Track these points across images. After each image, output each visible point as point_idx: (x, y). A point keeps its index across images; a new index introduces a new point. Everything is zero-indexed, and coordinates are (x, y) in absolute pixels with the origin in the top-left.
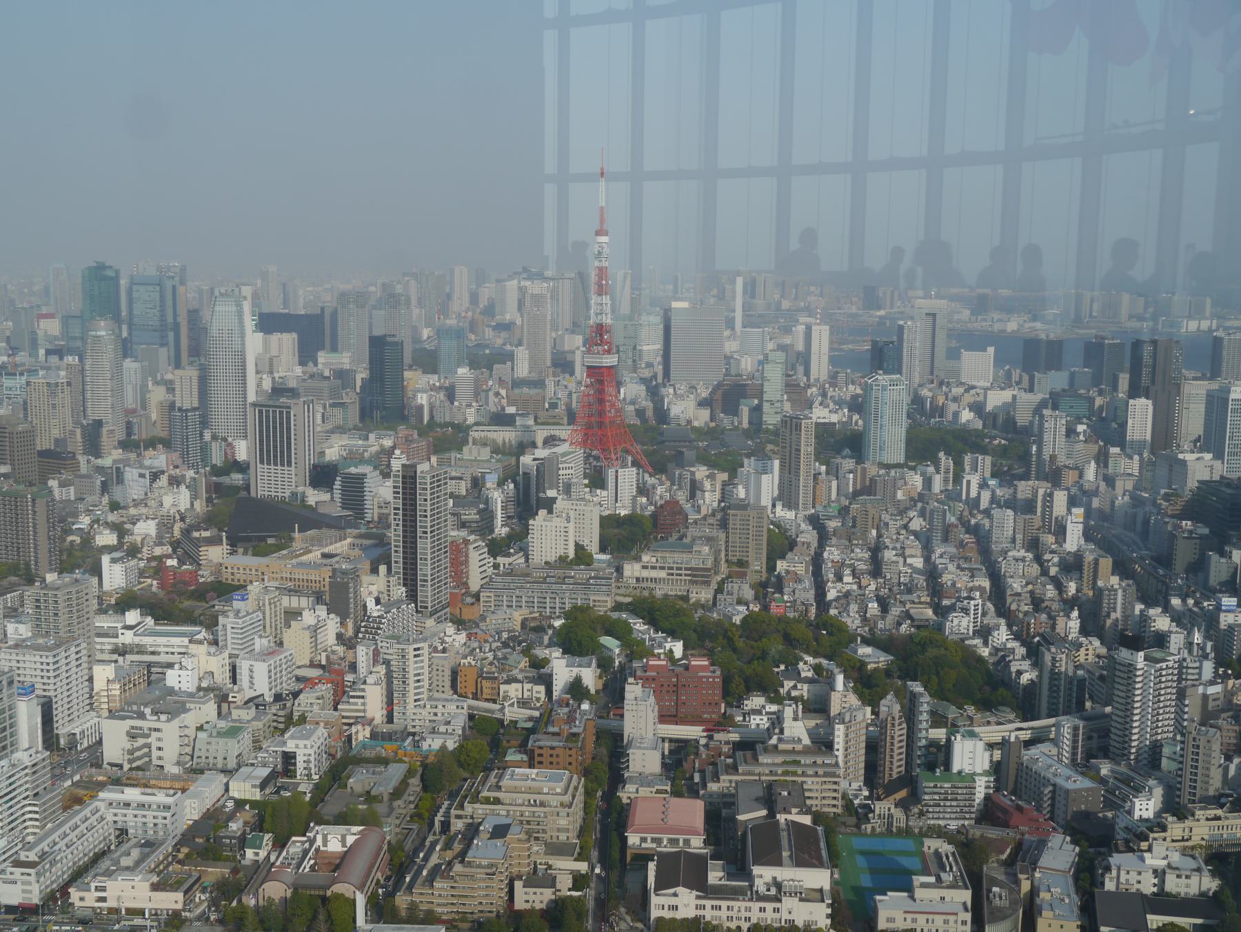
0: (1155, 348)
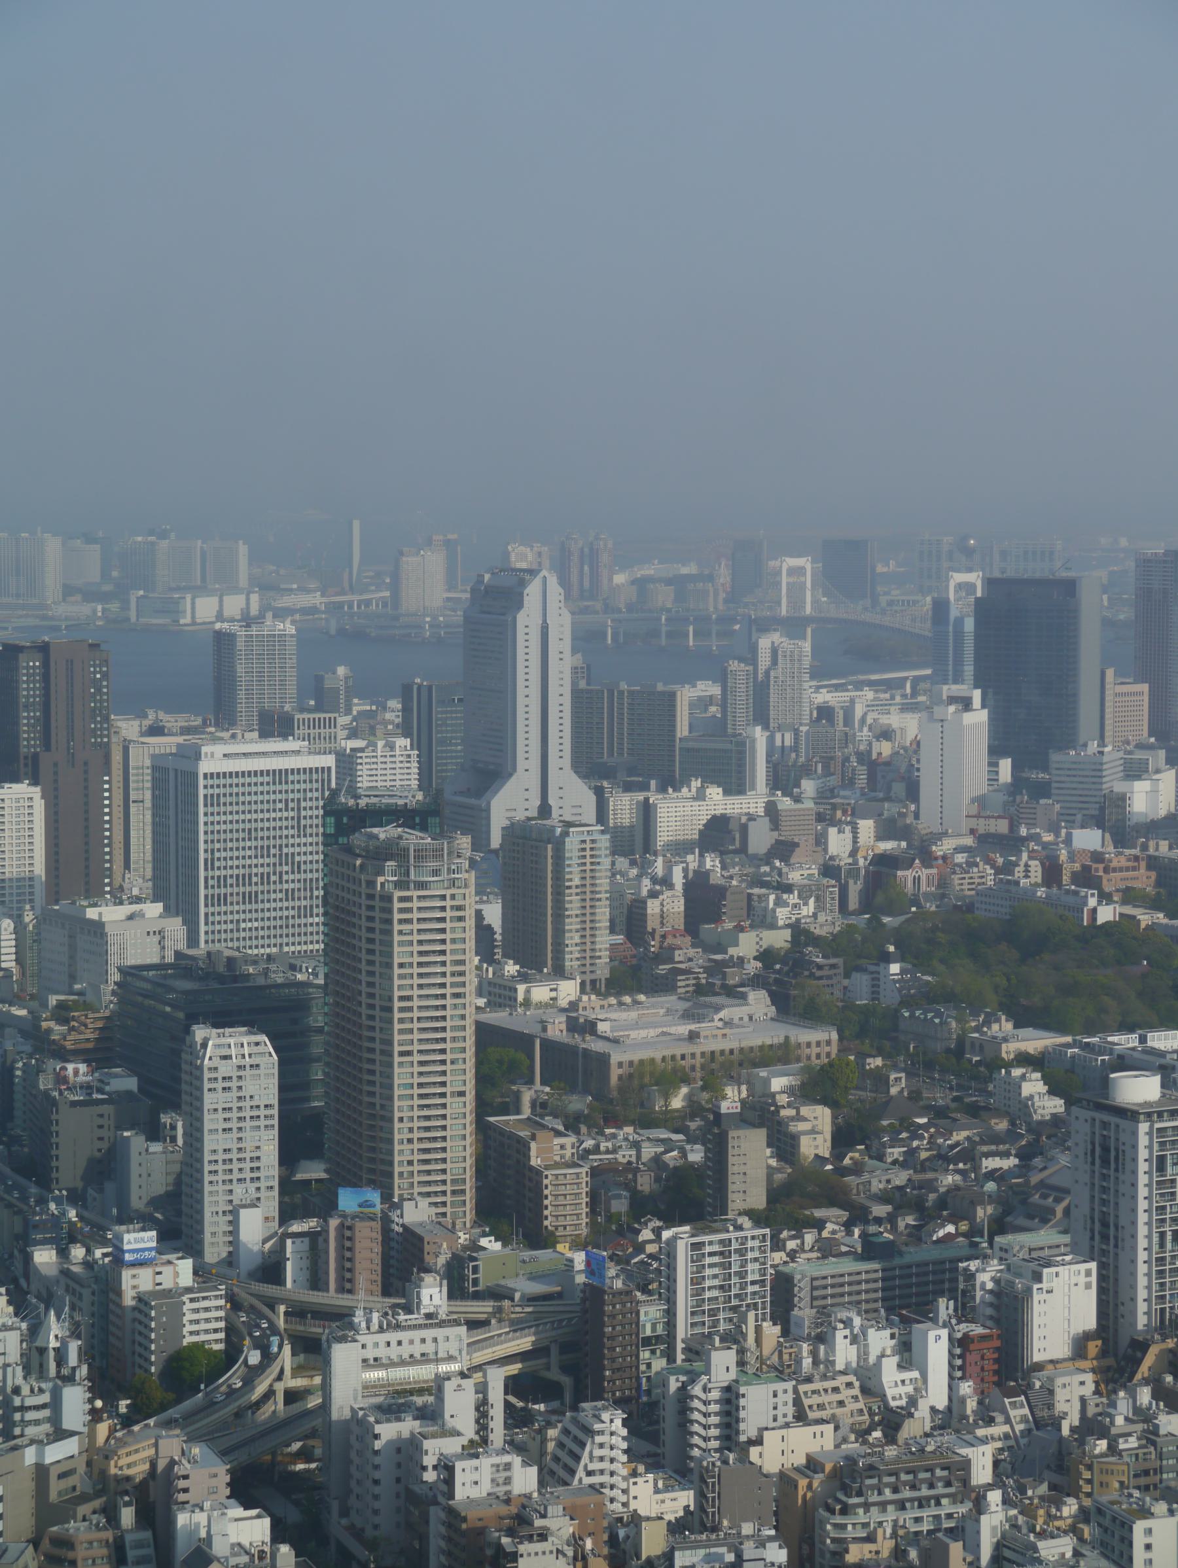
0: (46, 664)
